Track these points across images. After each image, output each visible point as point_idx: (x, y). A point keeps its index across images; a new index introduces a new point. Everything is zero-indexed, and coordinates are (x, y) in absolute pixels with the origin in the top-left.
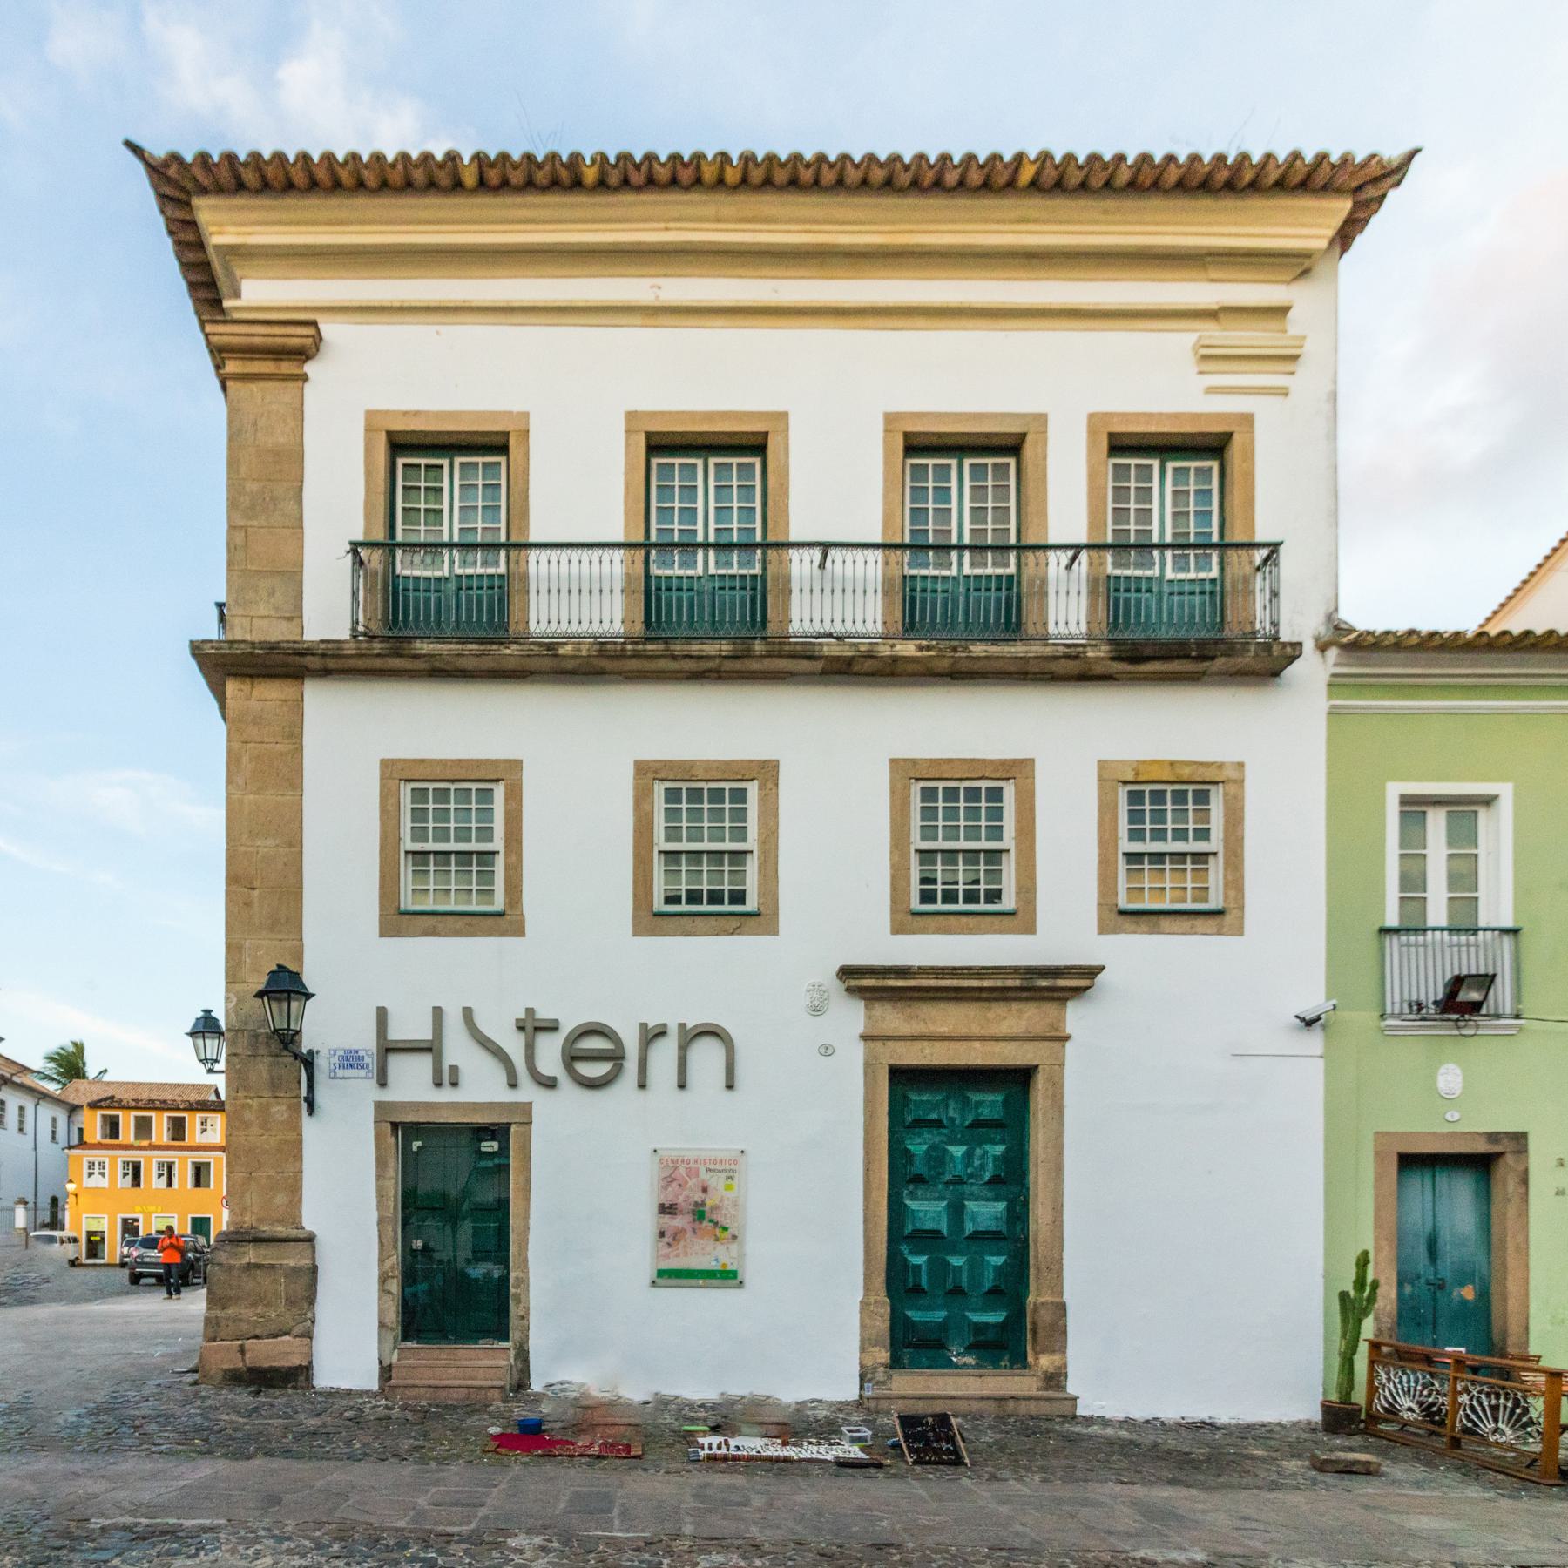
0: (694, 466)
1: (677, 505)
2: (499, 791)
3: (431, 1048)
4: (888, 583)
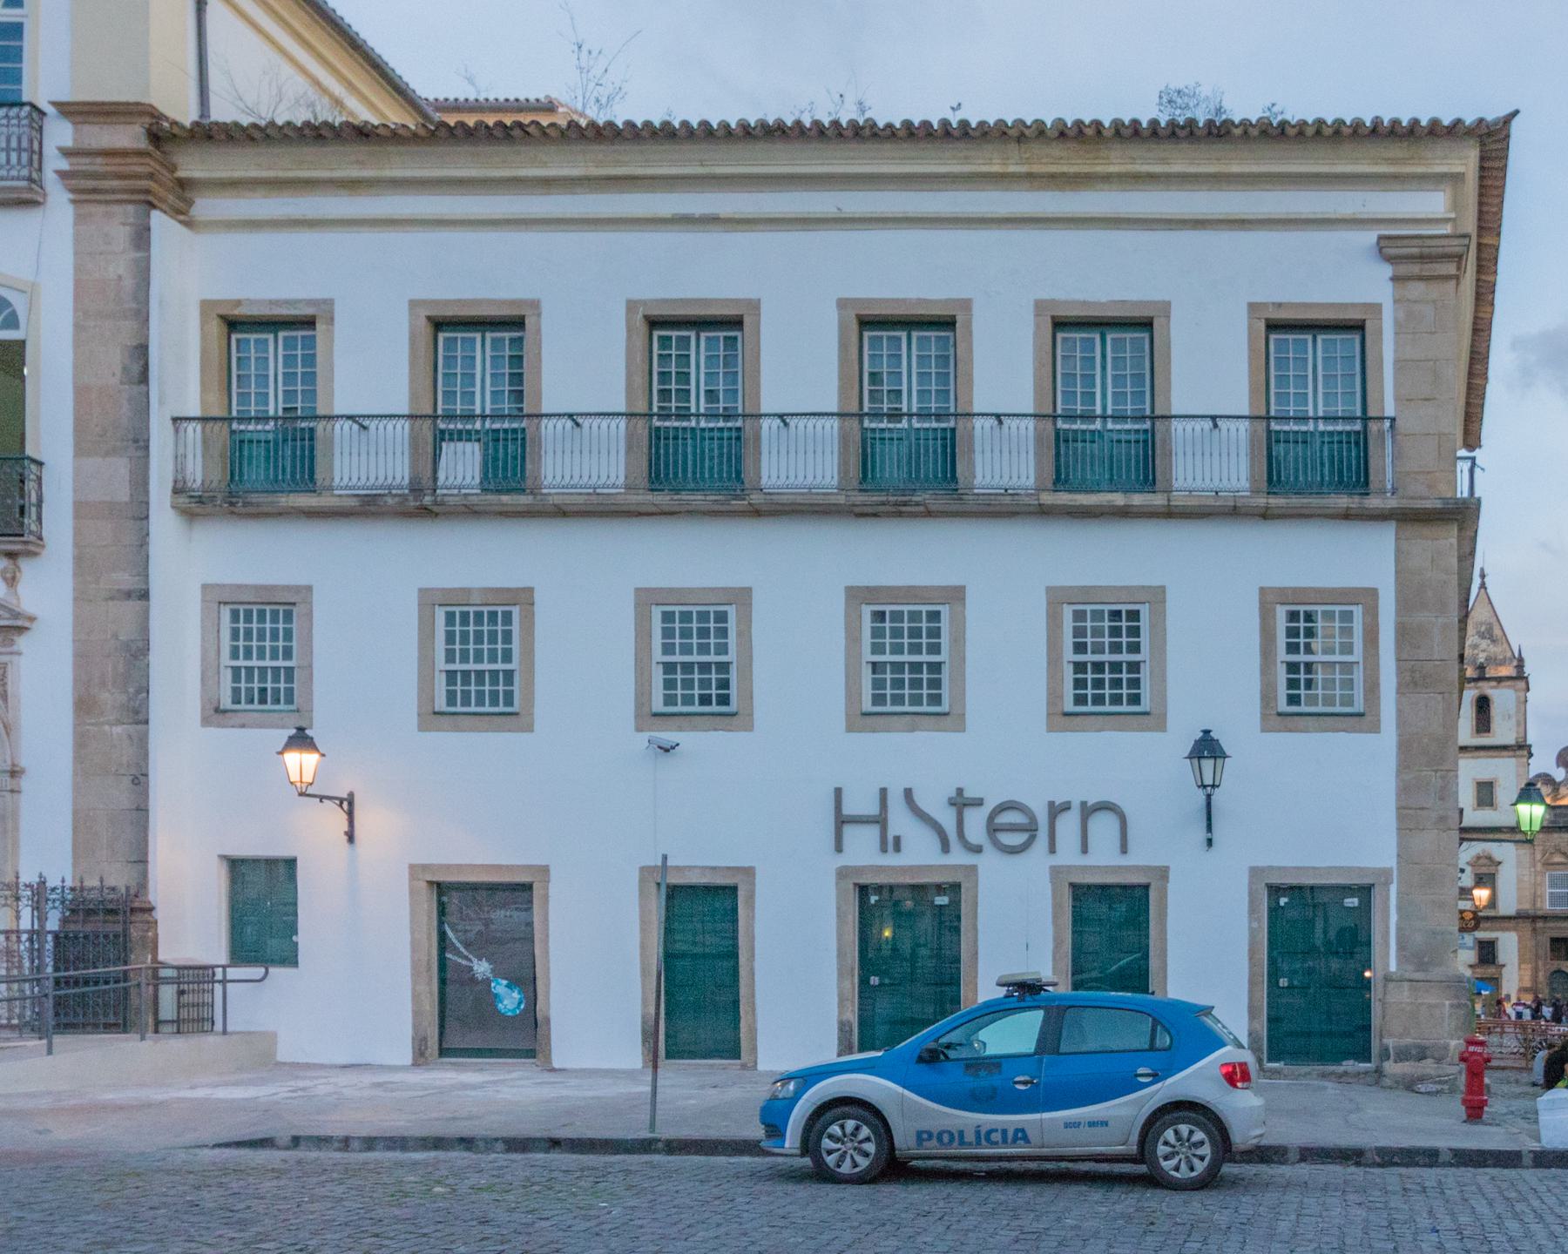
0: (899, 339)
1: (1292, 390)
2: (1357, 611)
3: (881, 821)
4: (1039, 439)
